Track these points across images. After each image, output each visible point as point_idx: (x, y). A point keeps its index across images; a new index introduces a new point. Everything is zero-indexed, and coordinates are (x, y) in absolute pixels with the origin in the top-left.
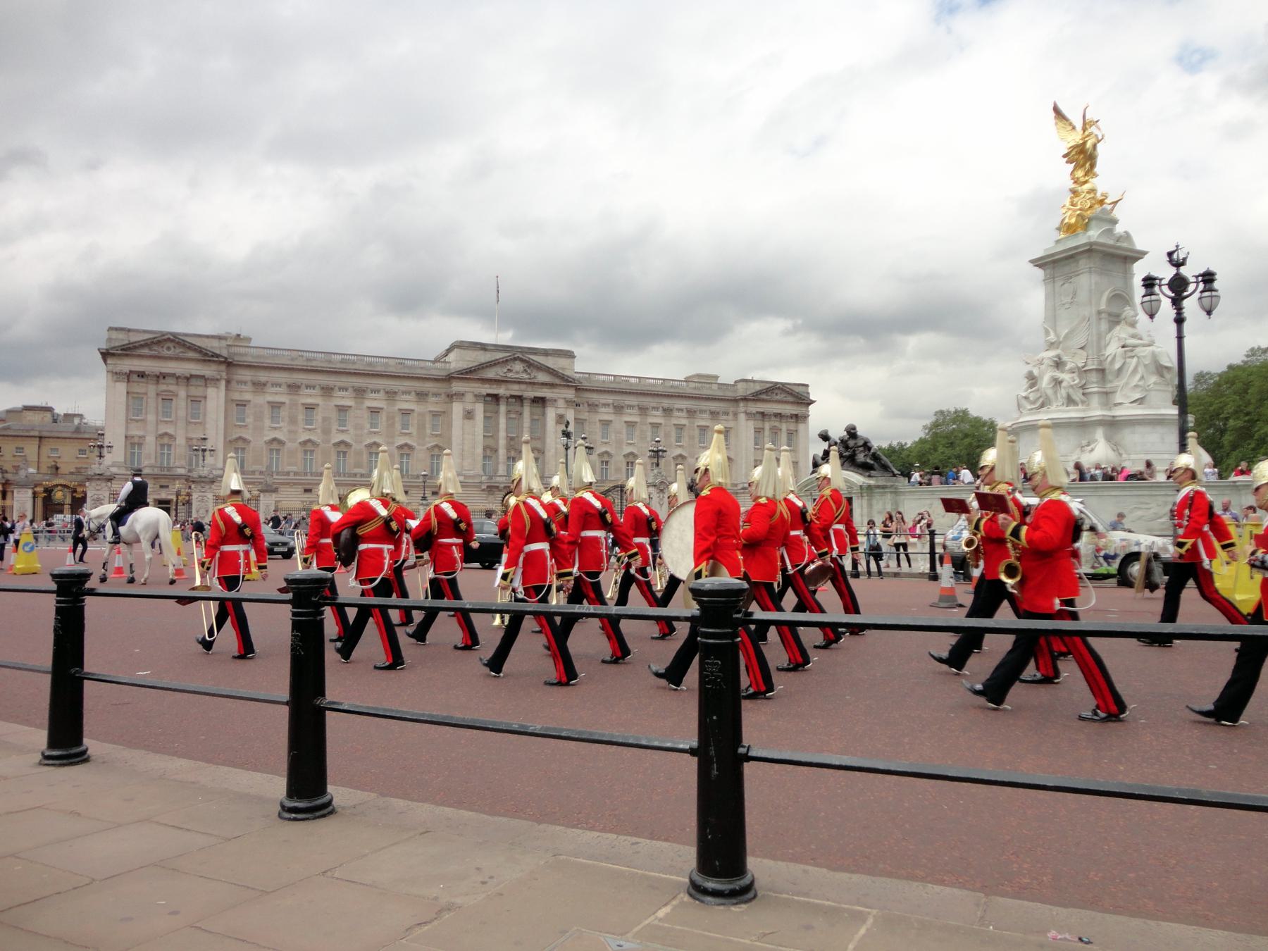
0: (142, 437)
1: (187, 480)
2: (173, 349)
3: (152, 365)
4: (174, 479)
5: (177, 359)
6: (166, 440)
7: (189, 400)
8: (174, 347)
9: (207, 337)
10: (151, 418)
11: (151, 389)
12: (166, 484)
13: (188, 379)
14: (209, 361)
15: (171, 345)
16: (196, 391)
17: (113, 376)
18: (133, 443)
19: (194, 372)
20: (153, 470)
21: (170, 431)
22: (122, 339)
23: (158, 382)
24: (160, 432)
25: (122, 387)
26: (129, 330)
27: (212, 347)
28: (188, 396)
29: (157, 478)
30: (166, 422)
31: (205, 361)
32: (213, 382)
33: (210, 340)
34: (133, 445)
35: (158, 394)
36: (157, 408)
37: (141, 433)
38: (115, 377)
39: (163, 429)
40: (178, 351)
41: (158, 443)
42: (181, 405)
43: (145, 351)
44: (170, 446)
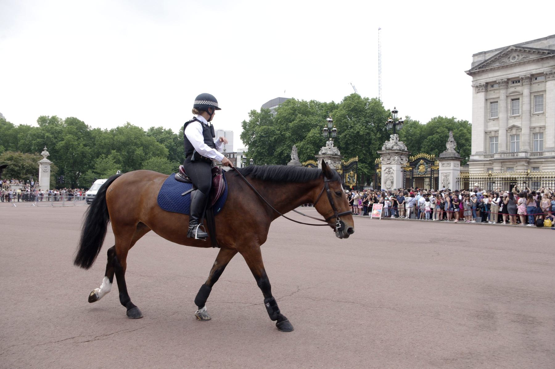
0: (496, 131)
1: (529, 163)
2: (517, 57)
3: (504, 74)
4: (516, 162)
5: (520, 64)
6: (514, 132)
7: (532, 97)
8: (518, 56)
9: (546, 38)
10: (502, 115)
11: (501, 94)
12: (512, 167)
13: (533, 78)
14: (547, 58)
15: (515, 54)
16: (536, 88)
17: (475, 90)
18: (491, 137)
19: (534, 72)
20: (501, 156)
21: (517, 123)
22: (481, 59)
23: (507, 88)
24: (510, 125)
25: (482, 96)
26: (485, 53)
27: (549, 46)
28: (531, 93)
29: (504, 162)
30: (515, 117)
31: (542, 59)
32: (552, 76)
33: (548, 40)
34: (491, 138)
35: (507, 96)
36: (507, 107)
37: (496, 128)
38: (477, 89)
39: (512, 122)
40: (519, 58)
41: (509, 134)
42: (525, 103)
43: (497, 64)
44: (518, 136)
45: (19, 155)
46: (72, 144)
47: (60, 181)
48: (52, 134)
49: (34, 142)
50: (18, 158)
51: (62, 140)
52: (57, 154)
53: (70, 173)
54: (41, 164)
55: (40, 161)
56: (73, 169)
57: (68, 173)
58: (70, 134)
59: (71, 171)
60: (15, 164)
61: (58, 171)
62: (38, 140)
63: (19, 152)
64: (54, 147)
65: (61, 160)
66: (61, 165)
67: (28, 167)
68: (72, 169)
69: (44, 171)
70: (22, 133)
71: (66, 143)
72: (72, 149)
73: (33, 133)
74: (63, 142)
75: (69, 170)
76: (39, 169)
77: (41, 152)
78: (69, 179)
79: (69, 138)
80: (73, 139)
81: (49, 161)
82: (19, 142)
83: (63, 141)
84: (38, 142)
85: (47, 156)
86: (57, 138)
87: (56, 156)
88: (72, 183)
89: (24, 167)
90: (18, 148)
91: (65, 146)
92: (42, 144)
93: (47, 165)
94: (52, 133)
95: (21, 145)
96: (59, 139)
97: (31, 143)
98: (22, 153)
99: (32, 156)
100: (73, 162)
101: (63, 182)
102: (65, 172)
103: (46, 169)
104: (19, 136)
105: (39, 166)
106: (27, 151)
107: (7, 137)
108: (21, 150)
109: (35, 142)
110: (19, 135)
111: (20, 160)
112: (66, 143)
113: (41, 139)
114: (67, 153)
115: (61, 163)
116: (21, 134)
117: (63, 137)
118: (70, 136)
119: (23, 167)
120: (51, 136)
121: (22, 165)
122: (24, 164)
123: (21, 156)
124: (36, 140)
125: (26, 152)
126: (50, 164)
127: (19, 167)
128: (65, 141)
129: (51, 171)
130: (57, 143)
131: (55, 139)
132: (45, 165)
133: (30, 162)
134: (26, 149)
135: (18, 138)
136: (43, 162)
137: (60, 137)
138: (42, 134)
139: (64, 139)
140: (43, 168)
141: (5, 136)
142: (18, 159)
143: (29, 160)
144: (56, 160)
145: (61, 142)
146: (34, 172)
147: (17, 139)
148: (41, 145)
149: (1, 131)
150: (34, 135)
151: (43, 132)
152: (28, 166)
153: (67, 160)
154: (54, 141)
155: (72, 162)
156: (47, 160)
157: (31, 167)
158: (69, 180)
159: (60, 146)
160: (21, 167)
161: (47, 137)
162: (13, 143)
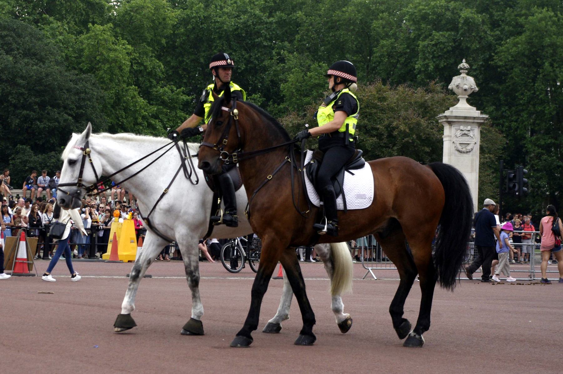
45: (377, 93)
46: (553, 45)
47: (514, 186)
48: (481, 12)
49: (421, 43)
50: (376, 104)
51: (518, 30)
52: (501, 82)
53: (545, 157)
54: (450, 123)
55: (447, 113)
56: (556, 139)
57: (538, 156)
58: (542, 6)
59: (547, 148)
60: (365, 127)
61: (504, 149)
62: (437, 35)
63: (379, 84)
64: (491, 58)
65: (513, 108)
66: (513, 124)
67: (406, 135)
68: (553, 141)
69: (460, 148)
70: (385, 14)
71: (530, 42)
72: (552, 65)
73: (420, 11)
74: (520, 37)
75: (543, 143)
76: (441, 142)
77: (449, 81)
78: (538, 179)
79: (540, 20)
80: (554, 23)
81: (474, 112)
82: (376, 47)
83: (520, 33)
84: (435, 45)
85: (470, 92)
86: (499, 26)
87: (497, 92)
88: (552, 194)
89: (395, 137)
90: (374, 69)
91: (527, 53)
92: (448, 52)
93: (469, 128)
94: (483, 9)
95: (382, 56)
96: (507, 28)
97: (413, 50)
98: (388, 87)
99: (419, 94)
100: (558, 114)
101: (525, 189)
102: (527, 153)
103: (465, 140)
104: (375, 24)
105: (441, 130)
106: (401, 80)
107: (338, 33)
108: (384, 75)
109: (426, 43)
110: (375, 21)
111: (383, 110)
112: (529, 43)
113: (448, 30)
114: (534, 80)
115: (514, 118)
116: (382, 19)
117: (521, 20)
118: (546, 12)
119: (390, 136)
120: (479, 18)
121: (387, 127)
122: (395, 124)
123: (384, 95)
124: (430, 35)
125: (398, 83)
126: (480, 124)
127: (379, 136)
128: (528, 33)
129: (482, 149)
130: (501, 45)
131: (492, 30)
132: (462, 127)
133: (414, 118)
134: (396, 70)
135: (373, 33)
136: (454, 114)
137: (508, 19)
138: (449, 14)
139: (522, 26)
140: (454, 140)
141: (332, 28)
142: (375, 107)
143: (410, 112)
144: (497, 110)
145: (512, 38)
146: (427, 153)
147: (369, 37)
148: (445, 53)
149: (321, 12)
150: (424, 17)
151: (452, 5)
152: (407, 130)
153: (534, 105)
154: (490, 35)
155: (554, 113)
156: (468, 106)
157: (414, 136)
158: (543, 183)
159: (510, 54)
160: (386, 135)
161: (467, 21)
162: (358, 51)
